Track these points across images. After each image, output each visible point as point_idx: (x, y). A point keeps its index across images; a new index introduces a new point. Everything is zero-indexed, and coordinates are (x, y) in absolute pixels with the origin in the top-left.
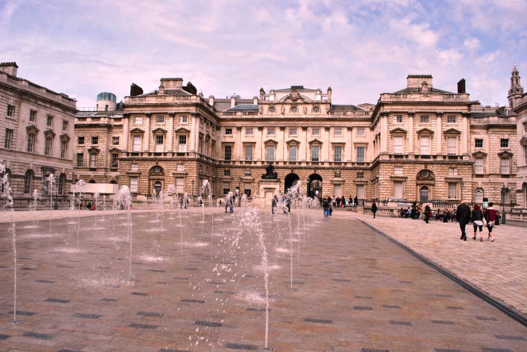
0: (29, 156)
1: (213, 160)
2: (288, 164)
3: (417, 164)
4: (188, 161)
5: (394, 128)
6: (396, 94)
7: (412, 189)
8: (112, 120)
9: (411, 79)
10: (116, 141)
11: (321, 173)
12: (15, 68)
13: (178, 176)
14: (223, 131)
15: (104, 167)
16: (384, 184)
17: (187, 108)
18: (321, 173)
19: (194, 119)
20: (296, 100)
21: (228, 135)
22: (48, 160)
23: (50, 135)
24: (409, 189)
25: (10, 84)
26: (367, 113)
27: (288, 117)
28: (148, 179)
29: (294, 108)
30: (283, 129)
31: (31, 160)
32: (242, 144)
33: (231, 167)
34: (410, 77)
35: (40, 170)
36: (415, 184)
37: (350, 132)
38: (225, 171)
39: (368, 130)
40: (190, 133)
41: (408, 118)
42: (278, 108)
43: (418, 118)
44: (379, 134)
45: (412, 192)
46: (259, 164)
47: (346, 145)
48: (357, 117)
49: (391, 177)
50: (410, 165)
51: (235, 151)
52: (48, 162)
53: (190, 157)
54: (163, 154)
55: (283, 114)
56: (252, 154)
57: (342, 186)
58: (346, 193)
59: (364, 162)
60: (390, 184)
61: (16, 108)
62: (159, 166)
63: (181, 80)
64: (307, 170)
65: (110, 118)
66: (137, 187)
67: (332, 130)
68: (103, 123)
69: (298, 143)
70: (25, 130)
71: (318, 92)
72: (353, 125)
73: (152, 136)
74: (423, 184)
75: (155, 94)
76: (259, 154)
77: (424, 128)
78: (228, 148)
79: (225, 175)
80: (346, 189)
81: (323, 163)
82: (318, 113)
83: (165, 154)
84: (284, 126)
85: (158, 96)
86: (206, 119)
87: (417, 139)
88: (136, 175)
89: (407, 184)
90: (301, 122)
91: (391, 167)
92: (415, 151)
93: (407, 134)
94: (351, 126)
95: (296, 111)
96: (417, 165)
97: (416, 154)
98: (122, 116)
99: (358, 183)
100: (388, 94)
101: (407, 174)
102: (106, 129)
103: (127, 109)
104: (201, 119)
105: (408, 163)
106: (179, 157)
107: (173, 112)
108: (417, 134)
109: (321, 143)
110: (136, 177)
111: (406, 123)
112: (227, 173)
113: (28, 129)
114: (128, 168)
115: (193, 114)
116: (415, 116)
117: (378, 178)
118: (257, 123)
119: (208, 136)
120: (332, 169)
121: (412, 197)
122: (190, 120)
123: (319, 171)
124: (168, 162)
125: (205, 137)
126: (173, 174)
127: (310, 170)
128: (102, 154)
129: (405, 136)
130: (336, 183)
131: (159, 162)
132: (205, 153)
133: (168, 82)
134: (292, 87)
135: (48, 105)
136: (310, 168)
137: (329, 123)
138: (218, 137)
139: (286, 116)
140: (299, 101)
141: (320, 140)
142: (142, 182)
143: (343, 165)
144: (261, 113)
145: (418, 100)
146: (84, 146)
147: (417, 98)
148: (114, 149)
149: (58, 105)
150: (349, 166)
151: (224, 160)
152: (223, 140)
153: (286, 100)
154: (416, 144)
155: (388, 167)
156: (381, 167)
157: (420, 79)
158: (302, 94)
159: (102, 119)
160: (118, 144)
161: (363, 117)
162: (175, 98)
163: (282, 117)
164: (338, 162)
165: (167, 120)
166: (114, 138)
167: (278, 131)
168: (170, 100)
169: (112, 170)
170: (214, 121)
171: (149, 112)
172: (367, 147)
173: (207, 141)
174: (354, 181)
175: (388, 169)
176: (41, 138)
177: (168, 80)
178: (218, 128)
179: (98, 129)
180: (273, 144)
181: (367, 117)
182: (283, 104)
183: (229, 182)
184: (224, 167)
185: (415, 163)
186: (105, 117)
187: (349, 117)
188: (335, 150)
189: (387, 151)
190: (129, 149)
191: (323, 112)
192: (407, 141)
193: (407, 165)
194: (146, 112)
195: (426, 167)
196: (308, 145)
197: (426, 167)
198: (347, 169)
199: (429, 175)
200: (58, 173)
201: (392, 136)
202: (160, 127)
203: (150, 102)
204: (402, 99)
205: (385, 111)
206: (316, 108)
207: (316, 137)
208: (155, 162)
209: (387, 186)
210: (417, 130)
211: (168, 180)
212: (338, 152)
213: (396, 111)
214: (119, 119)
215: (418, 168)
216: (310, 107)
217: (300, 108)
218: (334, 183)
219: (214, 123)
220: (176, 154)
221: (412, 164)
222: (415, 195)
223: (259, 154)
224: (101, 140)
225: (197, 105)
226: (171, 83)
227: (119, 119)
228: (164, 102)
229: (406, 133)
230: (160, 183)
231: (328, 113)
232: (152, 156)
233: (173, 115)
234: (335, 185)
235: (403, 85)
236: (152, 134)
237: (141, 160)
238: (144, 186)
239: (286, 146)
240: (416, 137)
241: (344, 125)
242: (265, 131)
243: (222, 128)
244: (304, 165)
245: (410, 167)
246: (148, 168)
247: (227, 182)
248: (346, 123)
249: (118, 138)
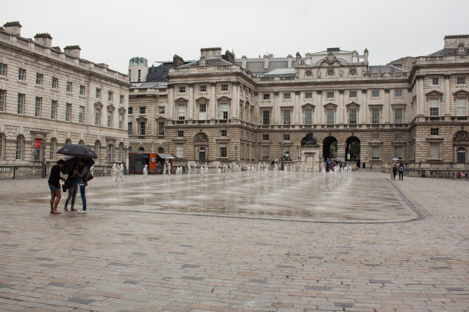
0: (96, 128)
1: (252, 125)
2: (326, 127)
3: (454, 125)
4: (230, 127)
5: (431, 90)
6: (433, 57)
7: (449, 151)
8: (158, 91)
9: (448, 40)
10: (161, 110)
11: (359, 135)
12: (79, 50)
13: (221, 142)
14: (261, 96)
15: (152, 135)
16: (421, 145)
17: (228, 77)
18: (359, 135)
19: (235, 88)
20: (332, 64)
21: (266, 100)
22: (110, 131)
23: (111, 108)
24: (446, 150)
25: (81, 67)
26: (405, 74)
27: (325, 80)
28: (193, 146)
29: (331, 72)
30: (319, 92)
31: (98, 132)
32: (280, 109)
33: (270, 131)
34: (446, 37)
35: (104, 140)
36: (452, 145)
37: (387, 94)
38: (264, 136)
39: (405, 91)
40: (231, 101)
41: (443, 80)
42: (314, 71)
43: (454, 80)
44: (416, 97)
45: (448, 153)
46: (297, 128)
47: (384, 107)
48: (395, 78)
49: (427, 139)
50: (446, 127)
51: (273, 116)
52: (111, 133)
53: (232, 124)
54: (206, 122)
55: (319, 78)
56: (290, 118)
57: (380, 148)
58: (384, 155)
59: (403, 123)
60: (426, 145)
61: (86, 88)
62: (204, 134)
63: (219, 49)
64: (345, 133)
65: (156, 89)
66: (182, 153)
67: (369, 92)
69: (335, 106)
70: (93, 106)
71: (355, 54)
72: (391, 87)
73: (195, 104)
74: (460, 145)
75: (197, 64)
76: (297, 118)
77: (460, 89)
78: (267, 113)
79: (264, 139)
80: (385, 151)
81: (360, 126)
82: (355, 76)
83: (208, 121)
84: (321, 89)
85: (200, 67)
86: (245, 86)
87: (453, 101)
88: (181, 142)
89: (443, 146)
90: (338, 86)
91: (426, 129)
92: (451, 113)
93: (443, 96)
94: (389, 87)
95: (333, 74)
96: (454, 127)
97: (453, 115)
98: (166, 87)
99: (397, 145)
100: (424, 57)
101: (443, 136)
103: (171, 80)
104: (241, 87)
105: (444, 125)
106: (222, 124)
107: (215, 81)
108: (453, 96)
109: (358, 106)
110: (183, 144)
111: (441, 85)
112: (266, 137)
113: (95, 105)
114: (174, 135)
115: (233, 83)
116: (451, 77)
117: (415, 140)
118: (294, 87)
119: (248, 103)
120: (370, 131)
121: (448, 158)
122: (230, 89)
123: (357, 133)
124: (212, 129)
125: (245, 103)
126: (216, 140)
127: (348, 133)
128: (150, 123)
129: (441, 98)
130: (374, 145)
131: (203, 129)
132: (244, 119)
133: (208, 52)
134: (328, 49)
135: (109, 83)
136: (348, 131)
137: (366, 85)
138: (257, 103)
139: (322, 80)
140: (335, 64)
141: (357, 102)
142: (188, 148)
143: (381, 127)
144: (298, 78)
145: (454, 62)
146: (133, 116)
147: (452, 60)
148: (161, 118)
149: (116, 82)
150: (387, 127)
151: (262, 124)
152: (261, 105)
153: (322, 63)
154: (453, 106)
155: (424, 129)
156: (417, 129)
157: (458, 40)
158: (338, 57)
159: (148, 90)
161: (401, 78)
162: (216, 68)
163: (319, 80)
164: (375, 124)
165: (209, 90)
166: (160, 107)
167: (315, 95)
168: (211, 70)
169: (159, 138)
170: (252, 87)
171: (192, 82)
172: (405, 108)
173: (246, 107)
174: (392, 143)
175: (424, 131)
176: (105, 111)
177: (208, 50)
178: (256, 94)
179: (145, 99)
180: (311, 108)
181: (404, 78)
182: (319, 67)
183: (268, 146)
184: (262, 132)
185: (451, 124)
186: (151, 88)
187: (386, 79)
188: (373, 111)
189: (423, 113)
190: (174, 117)
191: (360, 75)
192: (443, 103)
193: (443, 127)
194: (189, 82)
195: (462, 128)
196: (345, 108)
197: (462, 128)
198: (385, 131)
199: (466, 136)
201: (428, 98)
203: (193, 73)
204: (439, 62)
205: (420, 74)
206: (353, 70)
207: (353, 99)
208: (199, 129)
209: (423, 148)
210: (454, 92)
211: (212, 146)
212: (376, 114)
213: (431, 73)
214: (163, 90)
215: (454, 129)
216: (347, 70)
217: (336, 71)
218: (372, 145)
219: (252, 89)
220: (218, 122)
221: (448, 125)
222: (451, 155)
223: (297, 118)
225: (237, 74)
226: (211, 53)
227: (163, 90)
228: (206, 72)
229: (442, 95)
230: (204, 149)
231: (364, 75)
232: (196, 124)
233: (214, 84)
234: (373, 147)
235: (440, 46)
236: (195, 102)
237: (186, 128)
238: (190, 152)
239: (323, 110)
240: (453, 99)
241: (381, 87)
242: (303, 95)
243: (259, 93)
244: (341, 128)
245: (446, 129)
246: (192, 135)
247: (266, 146)
248: (384, 85)
249: (164, 107)
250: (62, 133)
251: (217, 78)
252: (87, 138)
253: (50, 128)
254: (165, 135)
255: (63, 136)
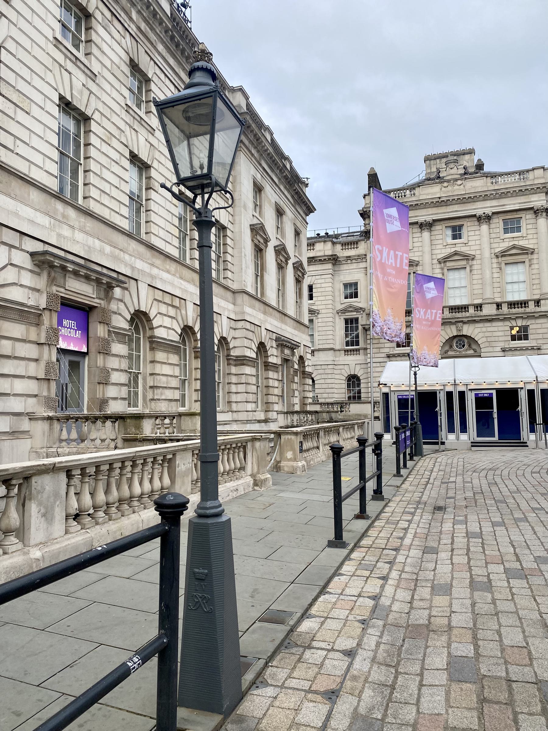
8: (339, 247)
68: (321, 254)
83: (479, 307)
102: (329, 266)
106: (514, 311)
124: (488, 324)
160: (356, 296)
200: (290, 358)
202: (458, 249)
208: (453, 328)
224: (319, 290)
250: (168, 299)
251: (494, 203)
252: (237, 334)
253: (126, 265)
254: (362, 344)
255: (172, 312)
